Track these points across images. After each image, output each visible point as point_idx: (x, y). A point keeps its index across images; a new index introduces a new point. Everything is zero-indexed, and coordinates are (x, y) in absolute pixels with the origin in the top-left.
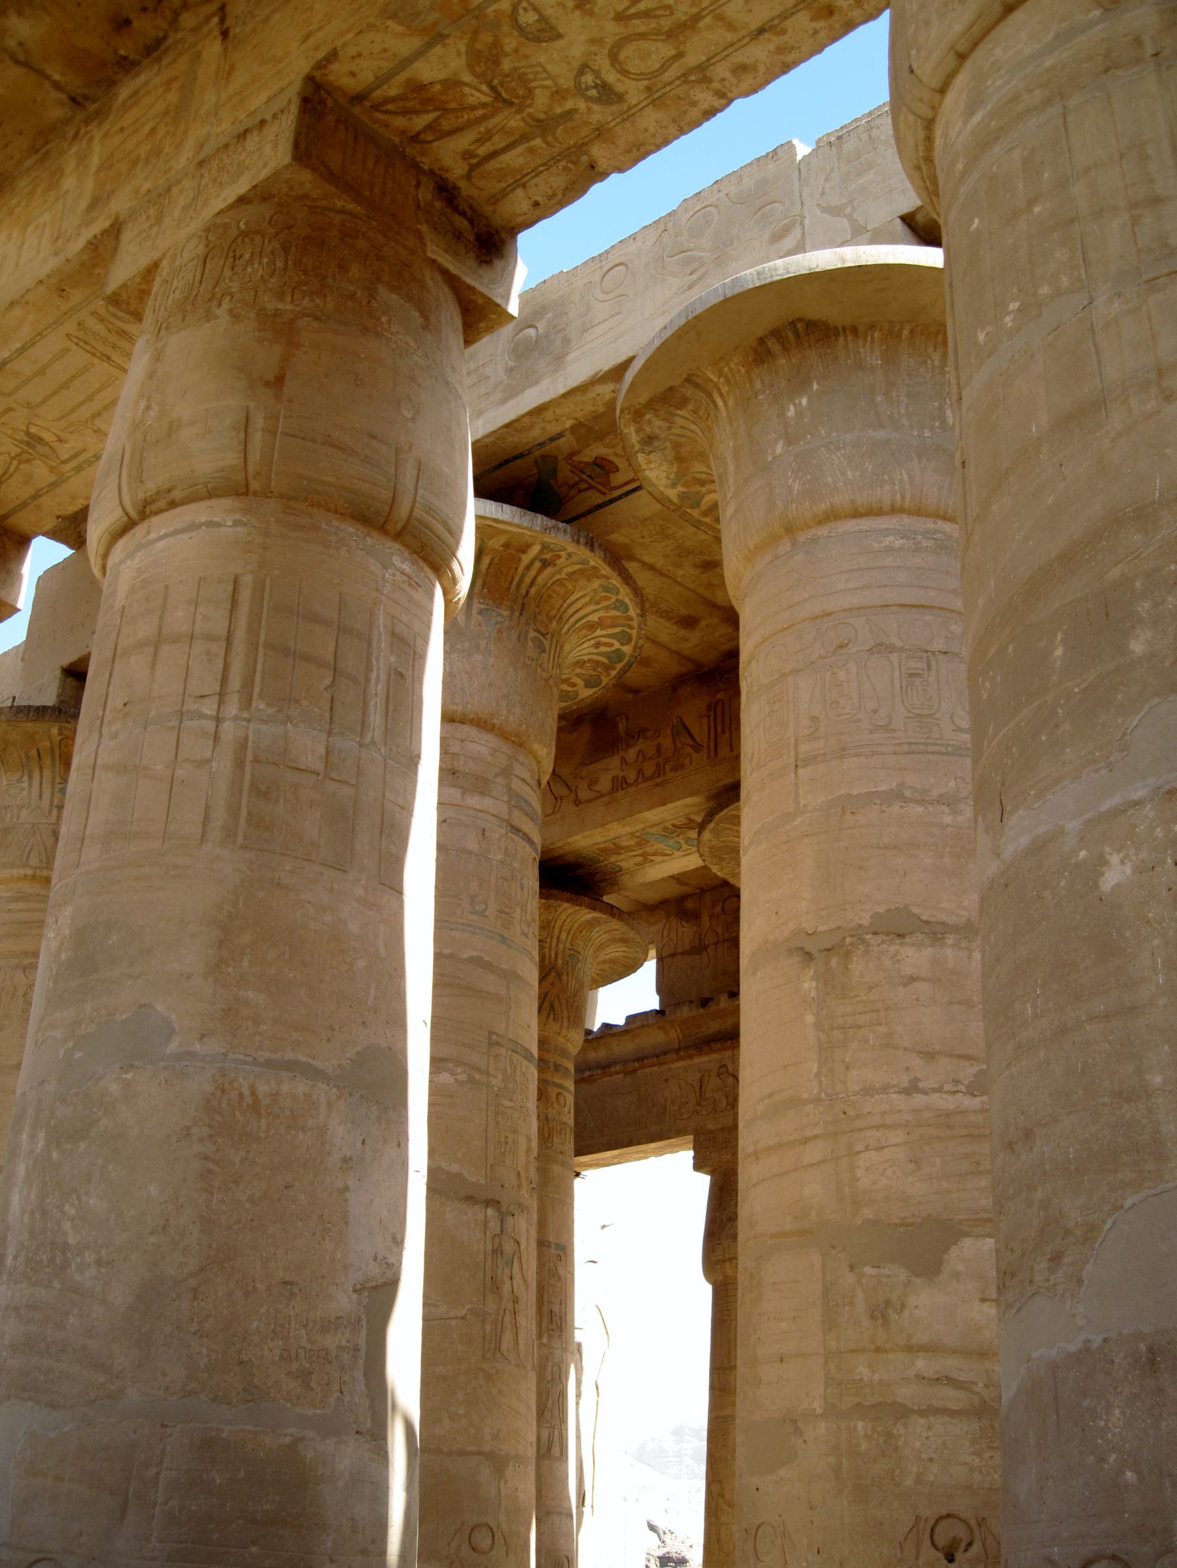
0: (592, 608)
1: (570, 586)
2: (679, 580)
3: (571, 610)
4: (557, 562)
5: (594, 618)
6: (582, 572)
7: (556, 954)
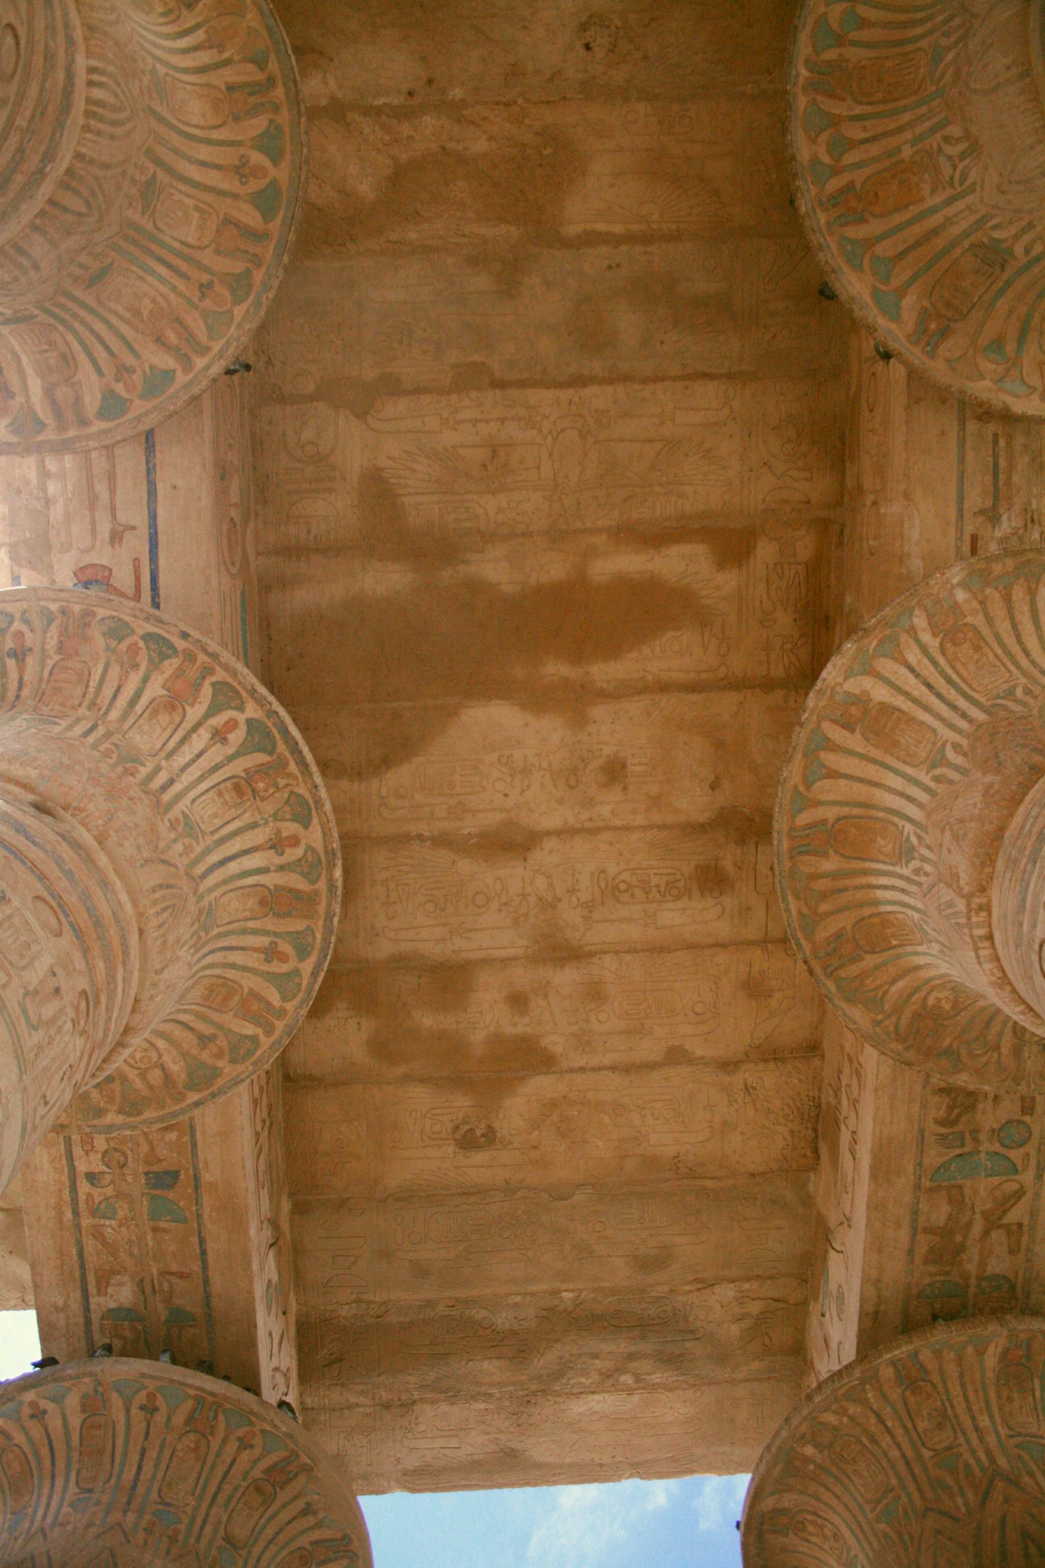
0: (134, 680)
1: (78, 666)
2: (618, 823)
3: (108, 692)
4: (29, 643)
5: (155, 689)
6: (64, 631)
7: (988, 1453)
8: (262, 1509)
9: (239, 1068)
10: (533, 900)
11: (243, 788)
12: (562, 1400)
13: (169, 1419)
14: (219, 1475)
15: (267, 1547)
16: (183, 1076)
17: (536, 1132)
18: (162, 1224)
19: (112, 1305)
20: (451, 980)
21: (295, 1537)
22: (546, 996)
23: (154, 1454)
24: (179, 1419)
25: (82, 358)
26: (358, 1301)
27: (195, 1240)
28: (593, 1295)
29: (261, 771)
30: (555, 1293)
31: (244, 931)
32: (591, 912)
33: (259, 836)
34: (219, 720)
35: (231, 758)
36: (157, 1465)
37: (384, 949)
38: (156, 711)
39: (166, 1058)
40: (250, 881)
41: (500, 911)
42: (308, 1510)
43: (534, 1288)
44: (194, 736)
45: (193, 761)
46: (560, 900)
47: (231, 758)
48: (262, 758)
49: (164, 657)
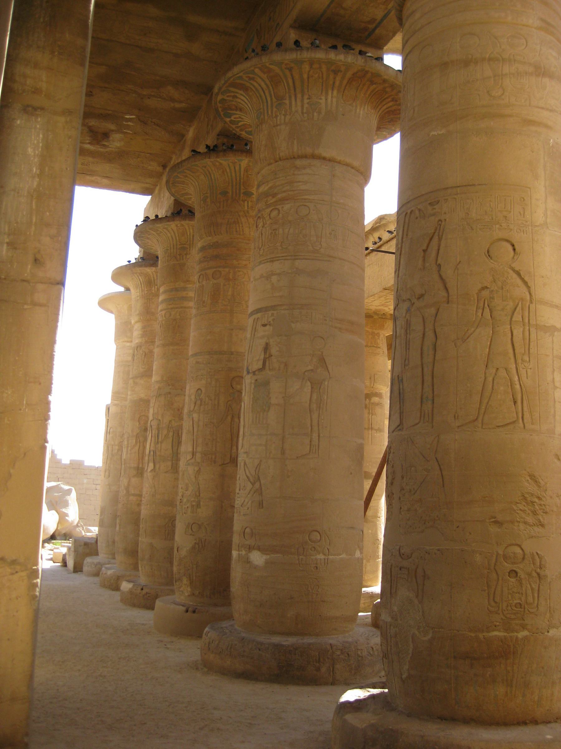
25: (242, 169)
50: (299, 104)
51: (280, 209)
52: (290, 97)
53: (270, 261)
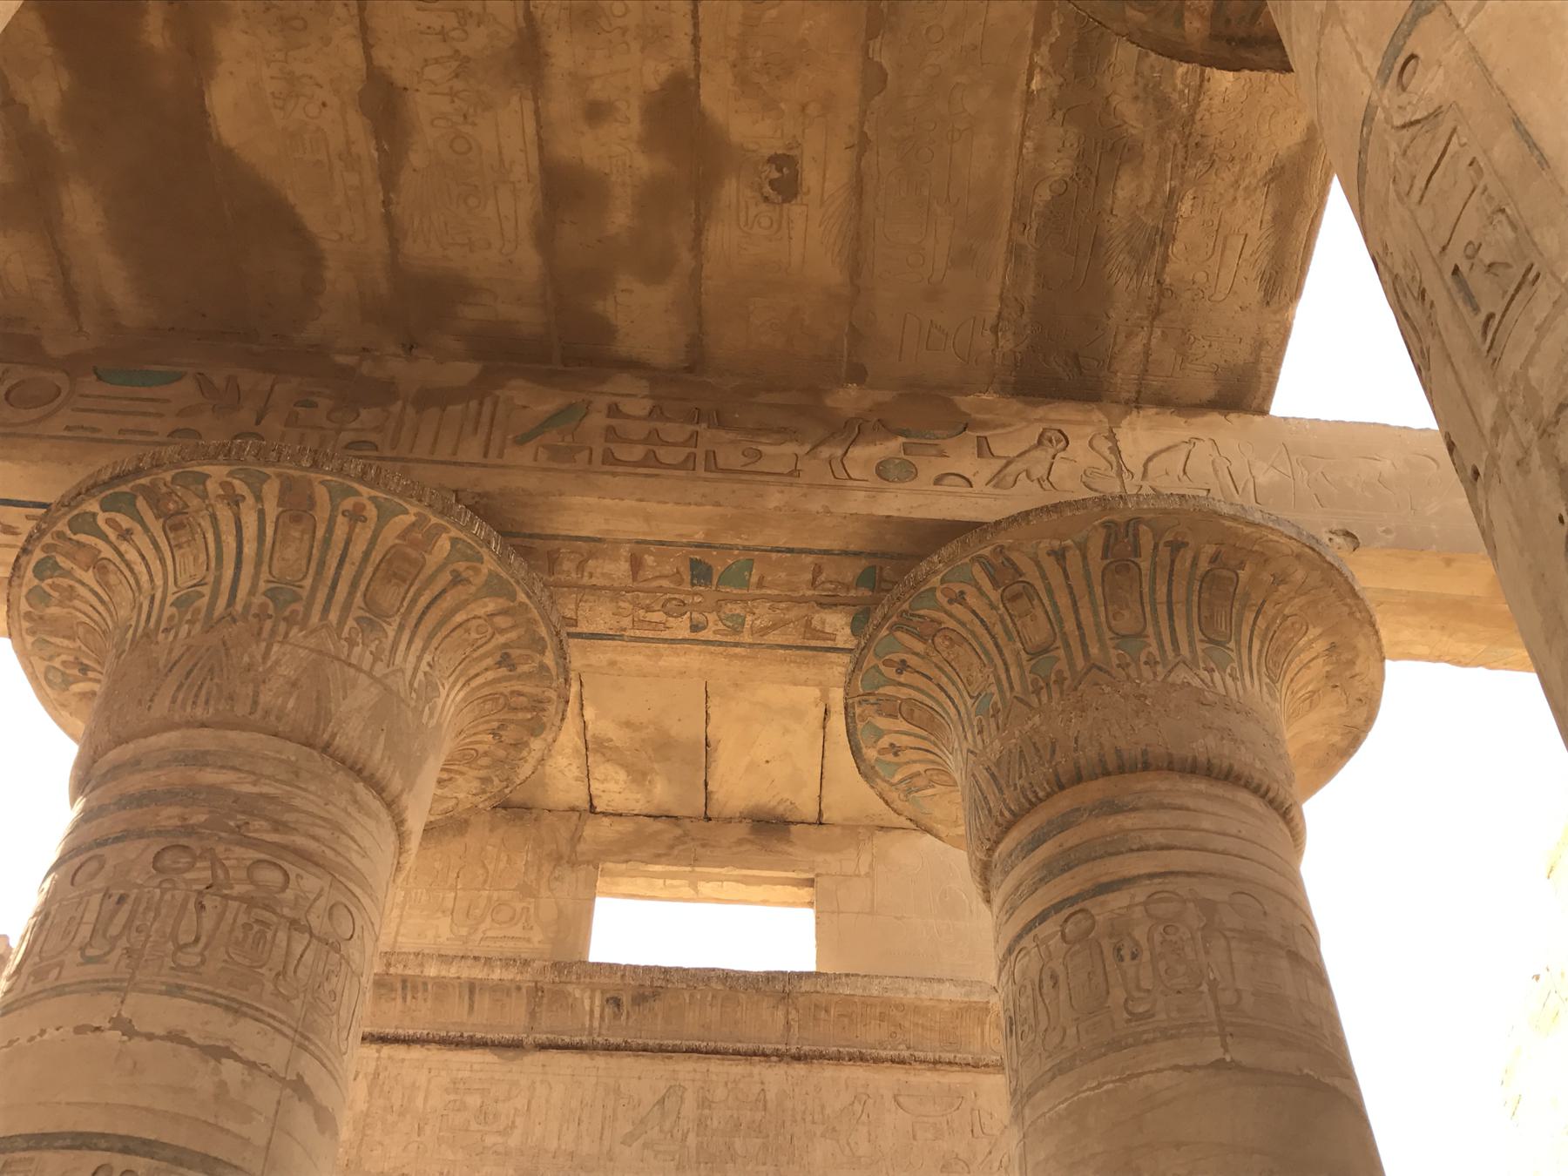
3: (96, 617)
5: (89, 577)
8: (1036, 602)
9: (486, 558)
10: (458, 85)
11: (176, 522)
12: (1206, 101)
13: (917, 654)
14: (981, 631)
15: (1076, 612)
16: (501, 601)
17: (783, 106)
18: (754, 579)
19: (848, 631)
20: (564, 190)
21: (1087, 576)
22: (591, 78)
23: (945, 679)
24: (919, 646)
26: (995, 329)
27: (774, 555)
28: (1044, 49)
29: (155, 502)
30: (1029, 97)
31: (327, 542)
32: (471, 14)
33: (225, 514)
34: (112, 536)
35: (146, 529)
36: (954, 683)
37: (529, 259)
38: (107, 584)
39: (481, 612)
40: (269, 531)
41: (474, 124)
42: (1060, 555)
43: (1016, 126)
44: (127, 557)
45: (147, 565)
46: (457, 51)
47: (146, 529)
48: (141, 503)
49: (56, 566)
50: (412, 659)
51: (292, 877)
52: (401, 627)
53: (227, 1008)
